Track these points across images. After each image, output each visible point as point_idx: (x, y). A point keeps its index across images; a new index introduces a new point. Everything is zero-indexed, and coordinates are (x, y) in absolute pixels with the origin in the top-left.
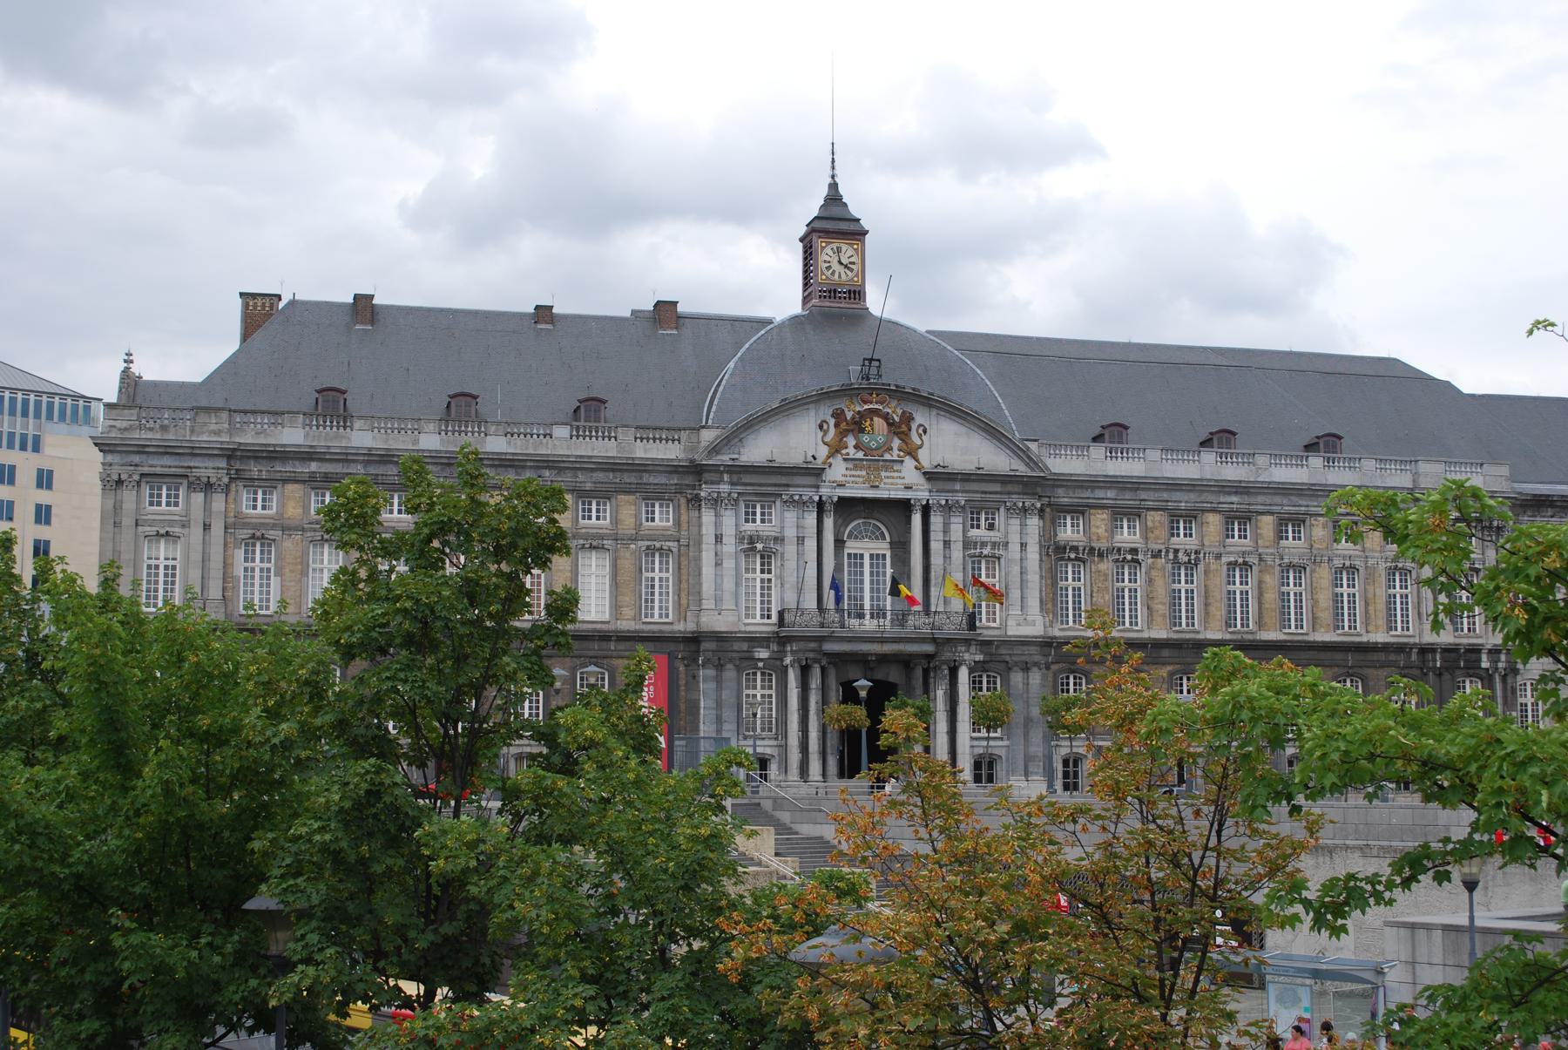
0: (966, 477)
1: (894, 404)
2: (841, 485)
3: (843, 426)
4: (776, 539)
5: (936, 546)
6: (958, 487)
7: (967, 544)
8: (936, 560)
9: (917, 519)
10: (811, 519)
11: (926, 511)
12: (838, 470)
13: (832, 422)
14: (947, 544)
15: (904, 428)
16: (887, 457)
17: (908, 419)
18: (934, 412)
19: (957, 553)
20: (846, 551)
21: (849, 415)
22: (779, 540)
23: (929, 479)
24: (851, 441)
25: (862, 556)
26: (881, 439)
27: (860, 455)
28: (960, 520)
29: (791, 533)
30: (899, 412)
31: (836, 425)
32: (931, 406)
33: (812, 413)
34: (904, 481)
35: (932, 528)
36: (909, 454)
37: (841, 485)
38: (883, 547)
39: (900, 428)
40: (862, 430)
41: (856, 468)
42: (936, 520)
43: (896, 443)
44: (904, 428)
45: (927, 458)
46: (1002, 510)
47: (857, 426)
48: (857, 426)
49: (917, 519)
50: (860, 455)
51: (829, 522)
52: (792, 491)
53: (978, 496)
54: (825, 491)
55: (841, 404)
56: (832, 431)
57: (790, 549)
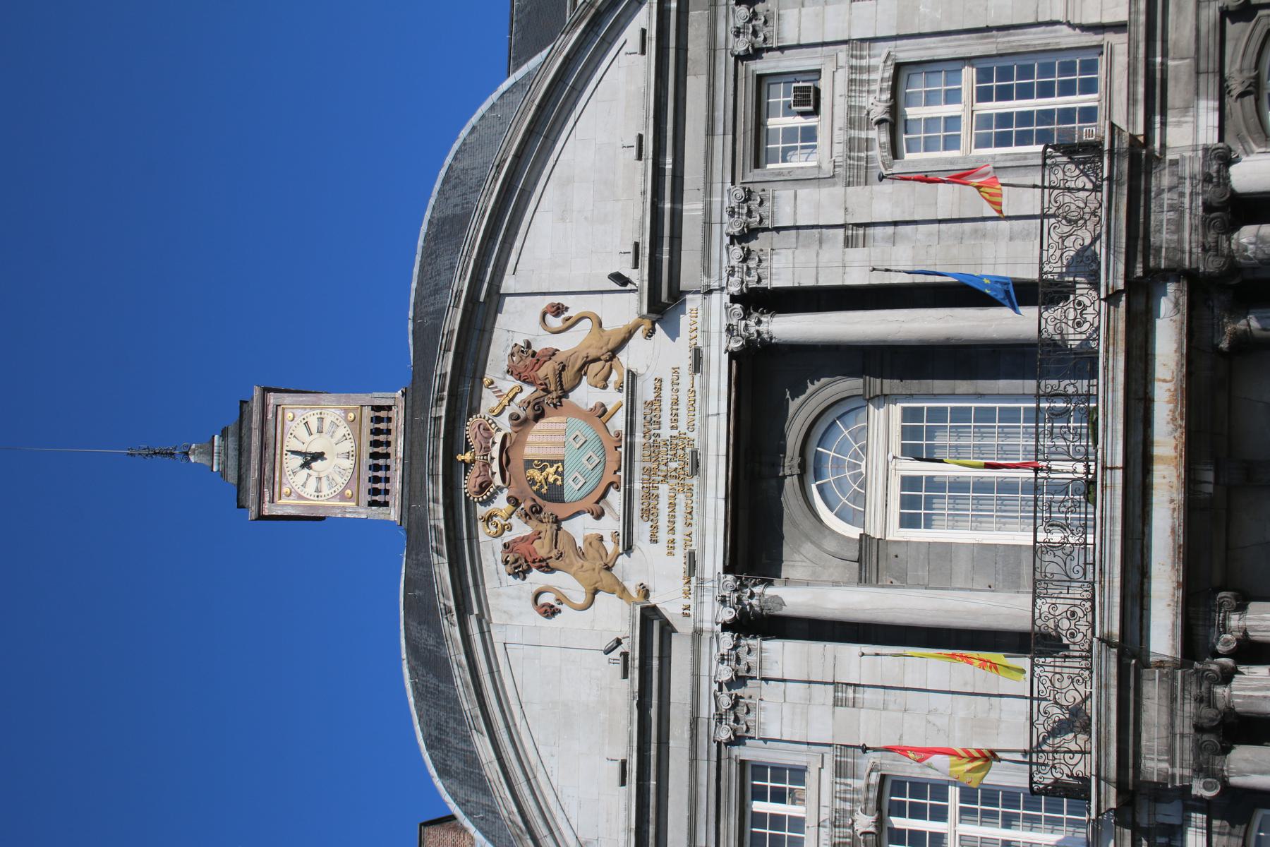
0: (665, 187)
1: (489, 401)
2: (692, 562)
3: (542, 549)
4: (840, 770)
5: (856, 271)
6: (692, 208)
7: (856, 172)
8: (899, 261)
9: (787, 327)
10: (781, 655)
11: (759, 300)
12: (657, 570)
13: (537, 578)
14: (855, 232)
15: (547, 370)
16: (618, 422)
17: (527, 361)
18: (509, 283)
19: (882, 201)
20: (896, 533)
21: (521, 529)
22: (845, 759)
23: (678, 296)
24: (580, 528)
25: (909, 483)
26: (580, 428)
27: (616, 499)
28: (784, 195)
29: (823, 723)
30: (509, 384)
31: (546, 567)
32: (496, 299)
33: (514, 636)
34: (685, 380)
35: (808, 281)
36: (614, 353)
37: (692, 562)
38: (884, 423)
39: (551, 386)
40: (555, 494)
41: (649, 513)
42: (786, 268)
43: (585, 395)
44: (547, 370)
45: (624, 310)
46: (759, 66)
47: (545, 502)
48: (545, 502)
49: (787, 327)
50: (616, 499)
51: (791, 597)
52: (707, 709)
53: (721, 143)
54: (713, 613)
55: (490, 550)
56: (560, 580)
57: (871, 725)
